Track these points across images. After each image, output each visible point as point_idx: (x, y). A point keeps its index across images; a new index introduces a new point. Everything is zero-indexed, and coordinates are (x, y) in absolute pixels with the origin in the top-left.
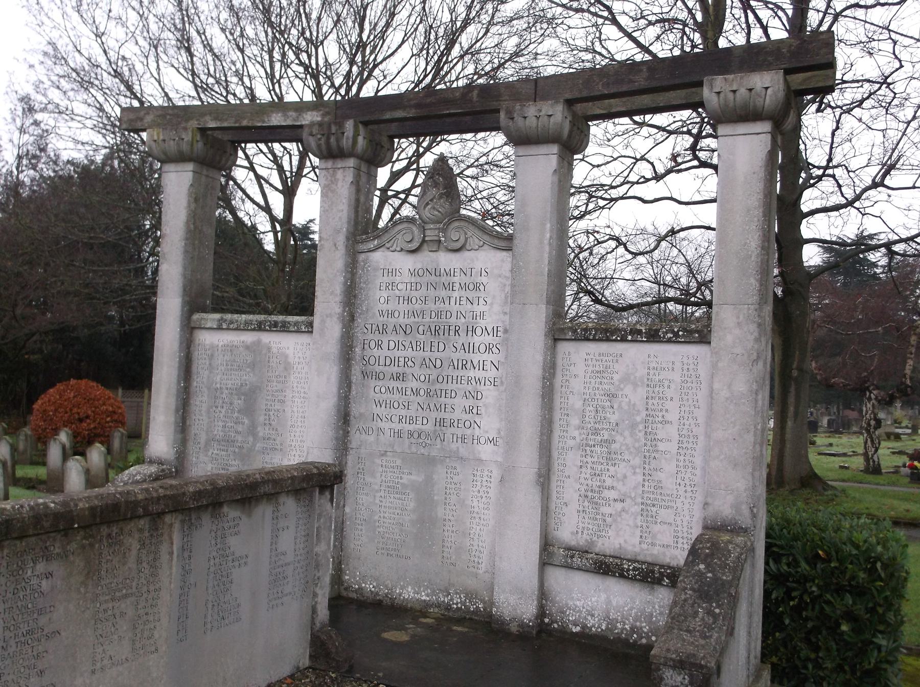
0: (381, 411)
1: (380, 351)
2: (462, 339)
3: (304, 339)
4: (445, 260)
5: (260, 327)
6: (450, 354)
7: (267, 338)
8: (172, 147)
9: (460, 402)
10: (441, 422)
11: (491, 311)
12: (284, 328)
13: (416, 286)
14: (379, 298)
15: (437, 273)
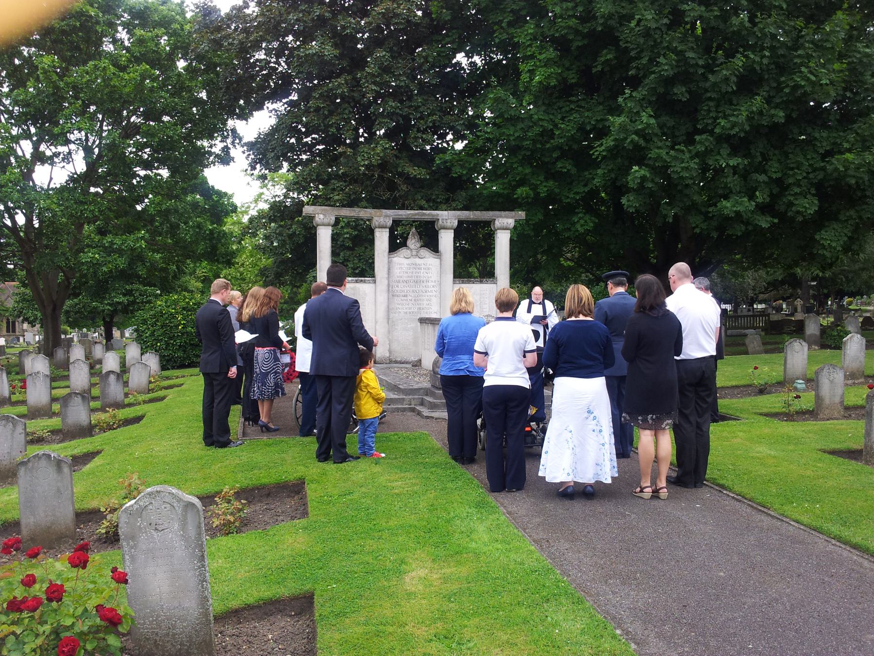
0: (400, 306)
1: (400, 288)
2: (424, 285)
3: (372, 285)
4: (418, 261)
5: (357, 282)
6: (421, 288)
7: (358, 285)
8: (326, 221)
9: (425, 302)
10: (420, 308)
11: (434, 275)
12: (364, 282)
13: (409, 269)
14: (397, 272)
15: (416, 264)
